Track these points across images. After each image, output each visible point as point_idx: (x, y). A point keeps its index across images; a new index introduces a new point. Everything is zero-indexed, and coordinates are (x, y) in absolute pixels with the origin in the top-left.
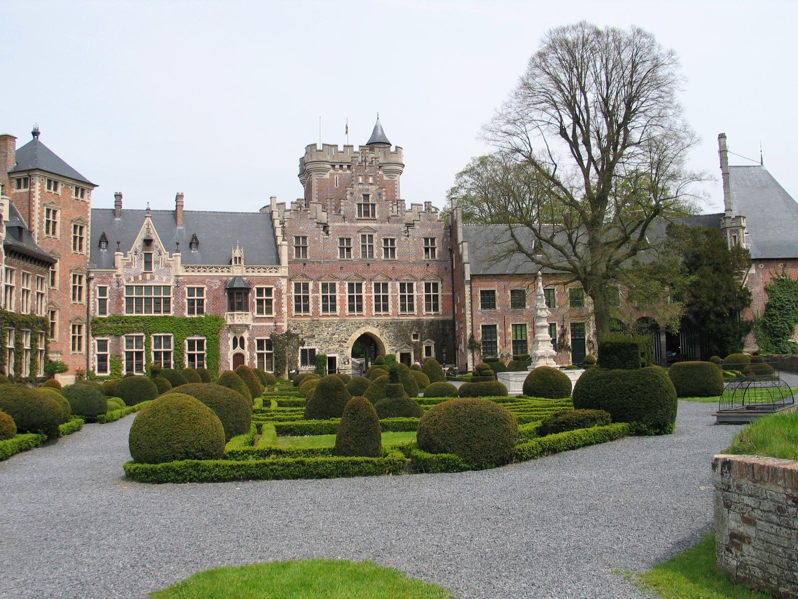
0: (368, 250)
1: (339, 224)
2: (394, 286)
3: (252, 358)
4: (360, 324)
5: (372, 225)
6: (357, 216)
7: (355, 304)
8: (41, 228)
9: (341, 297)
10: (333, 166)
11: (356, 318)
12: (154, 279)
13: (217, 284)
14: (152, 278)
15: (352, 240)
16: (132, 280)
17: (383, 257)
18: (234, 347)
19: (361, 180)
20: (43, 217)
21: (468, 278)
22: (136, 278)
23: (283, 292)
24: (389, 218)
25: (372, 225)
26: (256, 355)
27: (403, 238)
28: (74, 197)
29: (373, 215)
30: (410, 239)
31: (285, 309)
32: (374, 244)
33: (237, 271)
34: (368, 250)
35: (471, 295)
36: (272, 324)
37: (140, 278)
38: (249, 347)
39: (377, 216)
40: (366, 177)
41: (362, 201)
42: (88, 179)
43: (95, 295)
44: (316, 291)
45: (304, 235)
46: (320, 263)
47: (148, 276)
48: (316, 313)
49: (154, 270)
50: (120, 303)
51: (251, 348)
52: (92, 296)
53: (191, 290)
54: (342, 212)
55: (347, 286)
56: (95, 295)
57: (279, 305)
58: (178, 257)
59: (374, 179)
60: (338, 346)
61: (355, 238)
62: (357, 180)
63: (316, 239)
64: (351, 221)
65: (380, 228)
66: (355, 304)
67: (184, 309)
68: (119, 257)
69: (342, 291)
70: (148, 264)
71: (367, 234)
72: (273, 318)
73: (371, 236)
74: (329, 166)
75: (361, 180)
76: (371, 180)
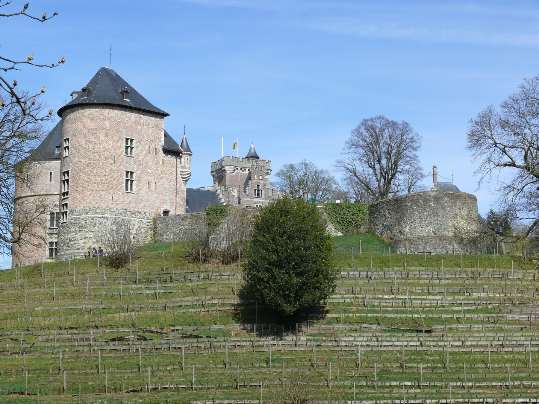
10: (237, 169)
25: (261, 200)
39: (263, 196)
40: (258, 176)
41: (256, 188)
54: (247, 193)
59: (262, 177)
62: (254, 177)
64: (251, 198)
76: (261, 177)
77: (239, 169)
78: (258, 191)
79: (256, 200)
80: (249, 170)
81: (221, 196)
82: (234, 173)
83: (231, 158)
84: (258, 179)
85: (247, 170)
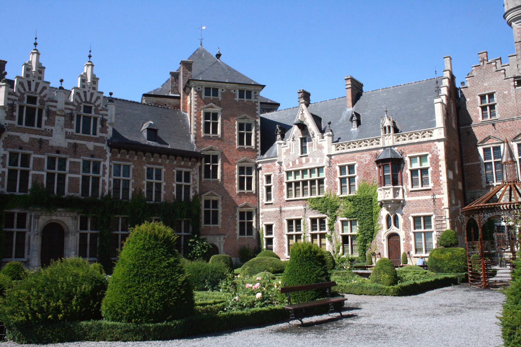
3: (408, 238)
8: (198, 129)
12: (308, 161)
13: (367, 158)
14: (307, 161)
16: (291, 165)
18: (389, 226)
20: (201, 119)
22: (294, 163)
23: (440, 158)
26: (412, 235)
28: (237, 99)
33: (389, 140)
36: (429, 197)
37: (297, 162)
38: (405, 225)
42: (255, 80)
43: (262, 183)
45: (490, 91)
46: (513, 120)
49: (308, 153)
51: (406, 226)
52: (260, 184)
53: (342, 168)
57: (436, 173)
63: (506, 92)
67: (336, 189)
70: (303, 149)
72: (430, 190)
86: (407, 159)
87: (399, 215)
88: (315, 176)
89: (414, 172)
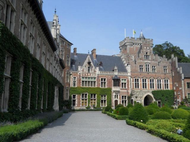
0: (147, 69)
1: (139, 61)
2: (156, 80)
3: (120, 102)
4: (146, 92)
5: (149, 62)
6: (144, 59)
7: (144, 86)
9: (141, 83)
11: (145, 90)
13: (110, 77)
14: (90, 75)
15: (143, 66)
16: (84, 75)
17: (152, 71)
18: (115, 98)
19: (145, 48)
21: (183, 78)
22: (85, 74)
24: (153, 60)
25: (149, 62)
27: (158, 66)
29: (149, 59)
30: (160, 66)
31: (130, 86)
32: (149, 67)
33: (116, 73)
34: (147, 69)
35: (184, 84)
36: (126, 91)
39: (150, 59)
40: (147, 48)
44: (133, 81)
47: (89, 74)
48: (133, 88)
50: (80, 83)
52: (71, 80)
53: (102, 79)
54: (140, 57)
55: (142, 80)
56: (72, 80)
57: (128, 85)
58: (98, 68)
59: (149, 48)
60: (140, 99)
61: (144, 65)
62: (144, 48)
64: (143, 60)
65: (151, 63)
66: (144, 86)
67: (100, 85)
68: (79, 68)
69: (141, 81)
70: (89, 70)
71: (147, 64)
73: (148, 65)
74: (133, 44)
75: (145, 48)
76: (148, 48)
77: (135, 44)
78: (147, 56)
79: (146, 61)
80: (140, 45)
81: (123, 59)
82: (132, 47)
83: (130, 38)
84: (146, 49)
85: (139, 44)
86: (121, 79)
87: (118, 95)
88: (93, 80)
89: (122, 83)
